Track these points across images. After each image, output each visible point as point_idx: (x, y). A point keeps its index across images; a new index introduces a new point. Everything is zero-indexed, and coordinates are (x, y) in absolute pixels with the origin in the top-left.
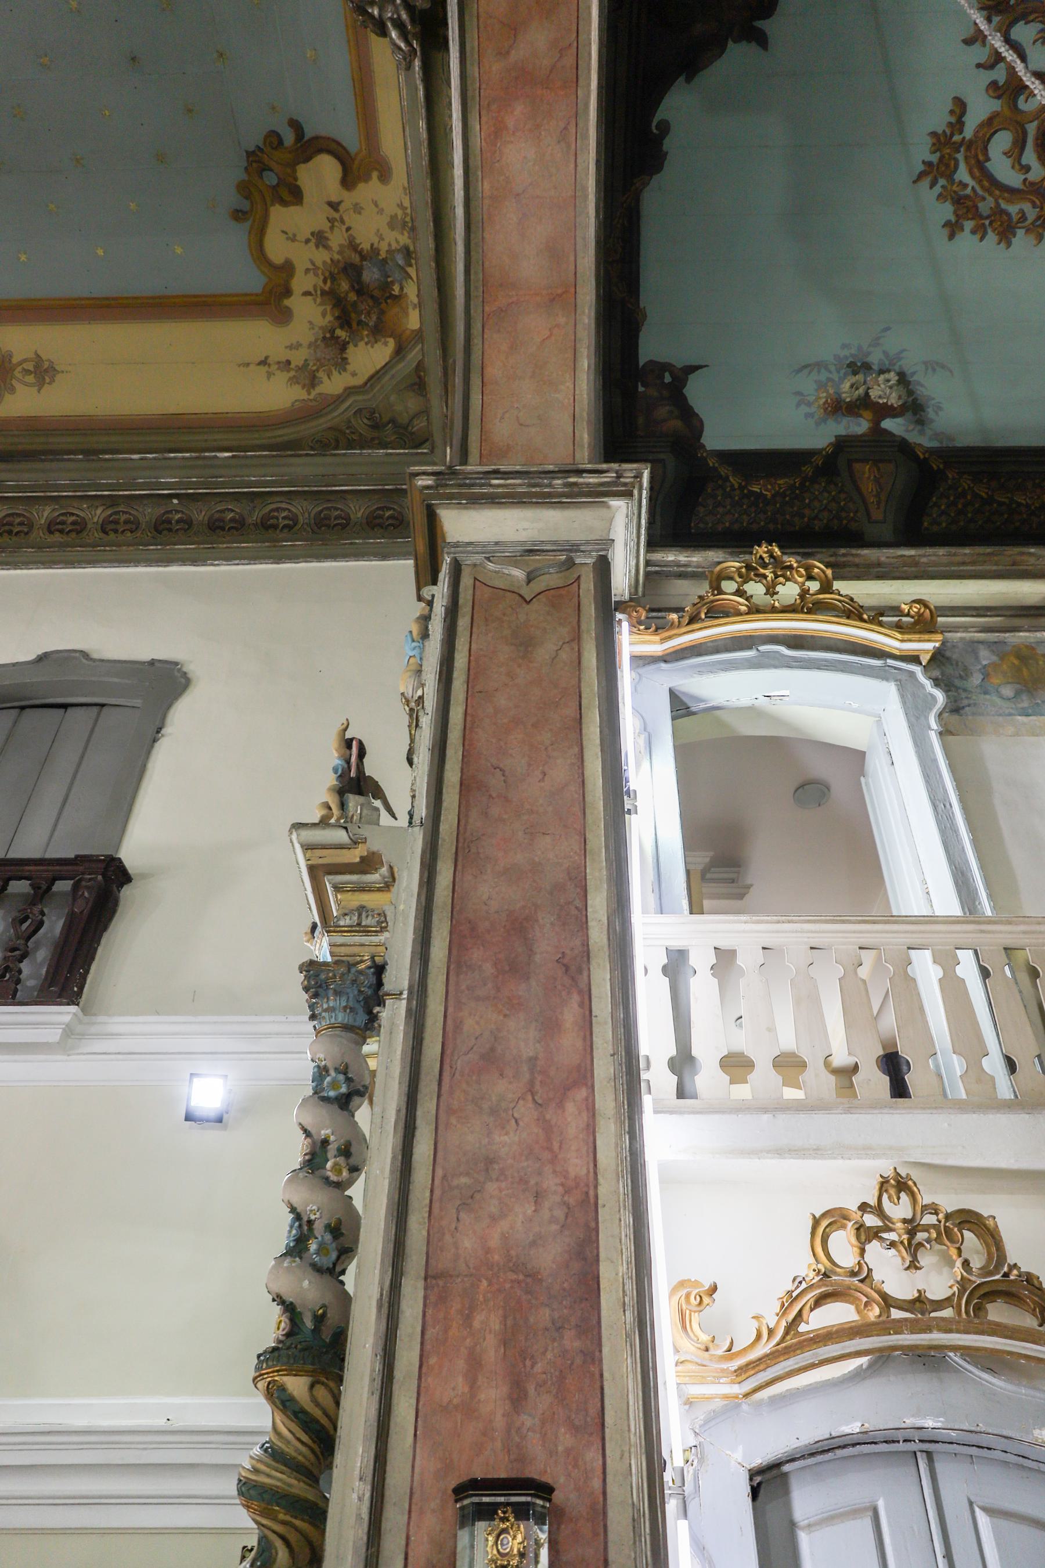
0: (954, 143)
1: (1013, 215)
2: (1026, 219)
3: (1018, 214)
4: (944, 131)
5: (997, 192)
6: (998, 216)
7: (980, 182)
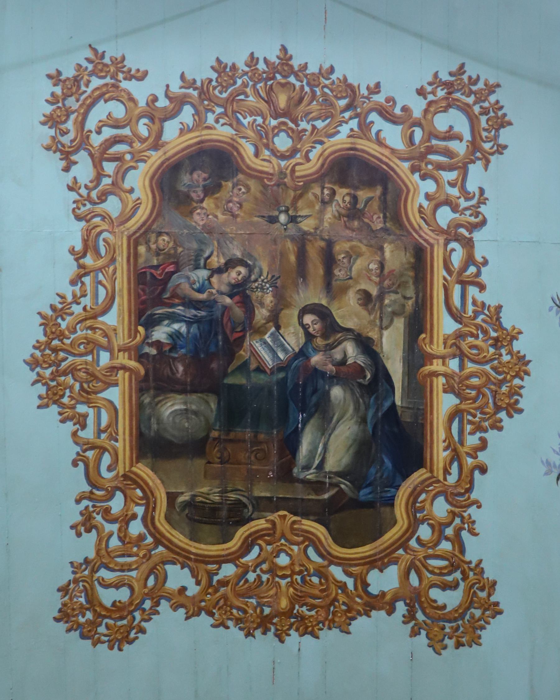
0: (117, 74)
1: (66, 125)
2: (62, 136)
3: (67, 129)
4: (125, 66)
5: (82, 111)
6: (65, 113)
7: (90, 96)
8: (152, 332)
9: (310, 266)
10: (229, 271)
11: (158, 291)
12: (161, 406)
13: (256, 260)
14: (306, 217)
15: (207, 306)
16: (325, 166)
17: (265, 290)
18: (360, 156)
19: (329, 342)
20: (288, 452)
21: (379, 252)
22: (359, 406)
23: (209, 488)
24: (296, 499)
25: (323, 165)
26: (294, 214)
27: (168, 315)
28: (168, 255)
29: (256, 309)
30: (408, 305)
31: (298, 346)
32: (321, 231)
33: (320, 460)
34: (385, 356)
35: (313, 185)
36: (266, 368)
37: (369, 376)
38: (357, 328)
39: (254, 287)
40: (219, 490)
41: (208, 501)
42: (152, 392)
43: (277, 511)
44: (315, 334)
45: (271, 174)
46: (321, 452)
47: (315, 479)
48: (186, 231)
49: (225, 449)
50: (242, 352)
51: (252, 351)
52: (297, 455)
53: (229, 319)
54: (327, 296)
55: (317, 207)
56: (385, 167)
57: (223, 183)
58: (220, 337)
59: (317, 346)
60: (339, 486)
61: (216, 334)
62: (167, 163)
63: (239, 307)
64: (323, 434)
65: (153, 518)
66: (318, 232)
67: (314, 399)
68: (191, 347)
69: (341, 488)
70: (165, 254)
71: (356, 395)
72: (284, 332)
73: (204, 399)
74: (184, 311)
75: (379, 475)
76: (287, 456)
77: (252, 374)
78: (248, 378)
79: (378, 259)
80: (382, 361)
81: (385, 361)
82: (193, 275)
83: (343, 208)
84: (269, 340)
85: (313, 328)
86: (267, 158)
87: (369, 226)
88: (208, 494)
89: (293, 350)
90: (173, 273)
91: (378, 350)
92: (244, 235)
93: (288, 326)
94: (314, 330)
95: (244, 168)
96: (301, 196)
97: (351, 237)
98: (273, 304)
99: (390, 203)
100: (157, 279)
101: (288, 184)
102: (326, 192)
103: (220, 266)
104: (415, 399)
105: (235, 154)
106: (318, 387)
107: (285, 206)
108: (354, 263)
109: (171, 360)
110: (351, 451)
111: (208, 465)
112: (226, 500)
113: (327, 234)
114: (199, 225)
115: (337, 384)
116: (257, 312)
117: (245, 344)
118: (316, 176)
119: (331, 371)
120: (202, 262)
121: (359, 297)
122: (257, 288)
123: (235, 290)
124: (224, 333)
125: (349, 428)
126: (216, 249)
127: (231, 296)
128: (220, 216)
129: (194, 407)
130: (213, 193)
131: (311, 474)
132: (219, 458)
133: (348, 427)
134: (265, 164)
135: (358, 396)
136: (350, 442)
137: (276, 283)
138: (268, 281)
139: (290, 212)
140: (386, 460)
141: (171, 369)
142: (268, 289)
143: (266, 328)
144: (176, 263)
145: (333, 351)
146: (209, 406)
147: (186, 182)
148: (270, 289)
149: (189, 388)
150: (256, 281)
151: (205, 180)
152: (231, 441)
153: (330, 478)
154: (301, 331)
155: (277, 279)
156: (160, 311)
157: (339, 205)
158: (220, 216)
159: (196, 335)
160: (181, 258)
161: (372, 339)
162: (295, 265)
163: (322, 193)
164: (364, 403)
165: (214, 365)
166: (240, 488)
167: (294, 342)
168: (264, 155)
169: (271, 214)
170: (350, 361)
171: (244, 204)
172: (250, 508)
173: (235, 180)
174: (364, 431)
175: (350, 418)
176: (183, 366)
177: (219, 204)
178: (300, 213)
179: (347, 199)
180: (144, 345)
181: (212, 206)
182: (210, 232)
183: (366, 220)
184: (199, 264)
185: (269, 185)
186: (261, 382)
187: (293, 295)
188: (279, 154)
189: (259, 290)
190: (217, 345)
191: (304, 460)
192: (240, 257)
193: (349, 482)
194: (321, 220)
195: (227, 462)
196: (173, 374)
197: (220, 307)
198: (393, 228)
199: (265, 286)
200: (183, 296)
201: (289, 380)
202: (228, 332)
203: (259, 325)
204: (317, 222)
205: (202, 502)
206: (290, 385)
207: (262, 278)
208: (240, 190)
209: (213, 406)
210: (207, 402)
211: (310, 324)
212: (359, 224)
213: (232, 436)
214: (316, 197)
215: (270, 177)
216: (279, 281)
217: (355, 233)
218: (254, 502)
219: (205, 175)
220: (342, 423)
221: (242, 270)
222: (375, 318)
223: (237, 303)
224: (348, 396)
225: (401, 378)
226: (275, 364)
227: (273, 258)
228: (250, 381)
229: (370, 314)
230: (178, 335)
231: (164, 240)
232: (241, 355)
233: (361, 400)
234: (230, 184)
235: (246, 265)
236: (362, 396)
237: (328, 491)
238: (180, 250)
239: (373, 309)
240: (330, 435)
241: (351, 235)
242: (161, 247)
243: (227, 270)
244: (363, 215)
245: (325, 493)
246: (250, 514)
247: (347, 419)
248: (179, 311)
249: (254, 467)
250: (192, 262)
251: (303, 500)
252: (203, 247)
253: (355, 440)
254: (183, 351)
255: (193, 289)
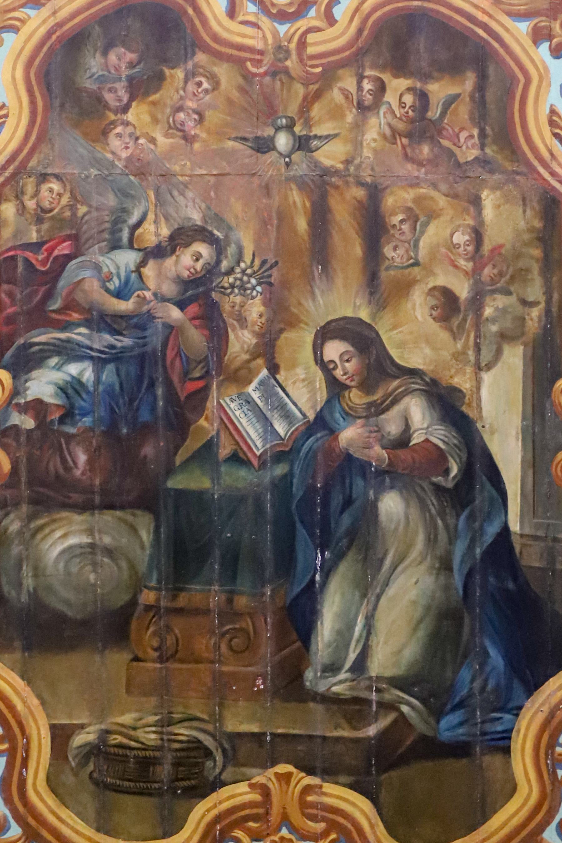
8: (26, 381)
9: (337, 239)
10: (177, 253)
11: (39, 297)
12: (43, 539)
13: (230, 228)
14: (328, 138)
15: (137, 326)
16: (366, 33)
17: (249, 292)
18: (432, 10)
19: (375, 398)
20: (294, 636)
21: (472, 209)
22: (436, 536)
23: (134, 715)
24: (311, 737)
25: (360, 31)
26: (304, 133)
27: (58, 346)
28: (59, 221)
29: (229, 330)
30: (532, 319)
31: (313, 407)
32: (358, 167)
33: (358, 651)
34: (487, 426)
35: (341, 72)
36: (250, 455)
37: (454, 470)
38: (431, 368)
39: (226, 285)
40: (157, 718)
41: (133, 744)
42: (24, 508)
43: (273, 764)
44: (348, 382)
45: (261, 53)
46: (361, 636)
47: (348, 694)
48: (94, 172)
49: (168, 628)
50: (202, 422)
51: (222, 419)
52: (313, 640)
53: (178, 354)
54: (370, 302)
55: (350, 118)
56: (481, 32)
57: (167, 72)
58: (160, 391)
59: (350, 408)
60: (398, 710)
61: (152, 385)
62: (58, 34)
63: (196, 327)
64: (364, 595)
65: (22, 782)
66: (352, 169)
67: (346, 520)
68: (102, 412)
69: (402, 714)
70: (52, 218)
71: (429, 511)
72: (286, 379)
73: (126, 522)
74: (89, 338)
75: (477, 685)
76: (294, 642)
77: (223, 469)
78: (216, 477)
79: (471, 222)
80: (482, 438)
81: (486, 438)
82: (108, 262)
83: (400, 119)
84: (255, 396)
85: (344, 368)
86: (252, 18)
87: (451, 154)
88: (135, 729)
89: (304, 415)
90: (69, 258)
91: (472, 413)
92: (208, 178)
93: (293, 365)
94: (345, 374)
95: (208, 39)
96: (318, 95)
97: (417, 178)
98: (263, 320)
99: (492, 107)
100: (37, 270)
101: (293, 73)
102: (367, 86)
103: (160, 242)
104: (548, 518)
105: (190, 11)
106: (354, 496)
107: (286, 117)
108: (422, 233)
109: (63, 441)
110: (421, 633)
111: (135, 664)
112: (169, 740)
113: (370, 172)
114: (120, 159)
115: (392, 488)
116: (232, 336)
117: (209, 405)
118: (347, 53)
119: (380, 460)
120: (125, 235)
121: (434, 302)
122: (232, 286)
123: (190, 293)
124: (169, 384)
125: (416, 583)
126: (152, 208)
127: (181, 305)
128: (161, 140)
129: (107, 540)
130: (147, 94)
131: (341, 682)
132: (156, 650)
133: (414, 580)
134: (249, 30)
135: (433, 511)
136: (418, 613)
137: (270, 276)
138: (254, 273)
139: (297, 129)
140: (493, 652)
141: (64, 461)
142: (254, 288)
143: (250, 370)
144: (75, 238)
145: (383, 416)
146: (139, 537)
147: (94, 70)
148: (259, 289)
149: (97, 499)
150: (230, 272)
151: (131, 65)
152: (180, 611)
153: (378, 691)
154: (319, 375)
155: (271, 267)
156: (42, 338)
157: (393, 112)
158: (161, 140)
159: (111, 386)
160: (85, 227)
161: (460, 391)
162: (306, 238)
163: (360, 88)
164: (446, 526)
165: (148, 450)
166: (199, 715)
167: (304, 400)
168: (248, 14)
169: (259, 134)
170: (416, 439)
171: (208, 114)
172: (219, 757)
173: (190, 65)
174: (447, 588)
175: (419, 559)
176: (86, 451)
177: (160, 116)
178: (316, 131)
179: (409, 99)
180: (10, 409)
181: (146, 118)
182: (141, 174)
183: (445, 143)
184: (120, 239)
185: (255, 75)
186: (241, 485)
187: (303, 301)
188: (274, 11)
189: (236, 291)
190: (153, 409)
191: (325, 653)
192: (199, 223)
193: (417, 699)
194: (358, 145)
195: (172, 657)
196: (68, 469)
197: (160, 326)
198: (499, 157)
199: (249, 282)
200: (87, 307)
201: (295, 481)
202: (175, 379)
203: (237, 363)
204: (349, 147)
205: (120, 746)
206: (298, 490)
207: (243, 265)
208: (200, 84)
209: (146, 536)
210: (133, 529)
211: (338, 361)
212: (432, 150)
213: (182, 601)
214: (347, 97)
215: (258, 57)
216: (275, 273)
217: (423, 170)
218: (227, 746)
219: (131, 56)
220: (403, 571)
221: (203, 249)
222: (466, 346)
223: (193, 319)
224: (415, 513)
225: (520, 474)
226: (268, 446)
227: (265, 223)
228: (219, 483)
229: (455, 339)
230: (77, 387)
231: (51, 190)
232: (202, 428)
233: (439, 522)
234: (180, 74)
235: (211, 240)
236: (442, 514)
237: (376, 721)
238: (82, 210)
239: (461, 326)
240: (379, 597)
241: (416, 174)
242: (46, 204)
243: (173, 251)
244: (440, 132)
245: (370, 725)
246: (217, 771)
247: (412, 562)
248: (79, 338)
249: (225, 669)
250: (106, 236)
251: (324, 738)
252: (128, 204)
253: (428, 608)
254: (87, 421)
255: (107, 290)
